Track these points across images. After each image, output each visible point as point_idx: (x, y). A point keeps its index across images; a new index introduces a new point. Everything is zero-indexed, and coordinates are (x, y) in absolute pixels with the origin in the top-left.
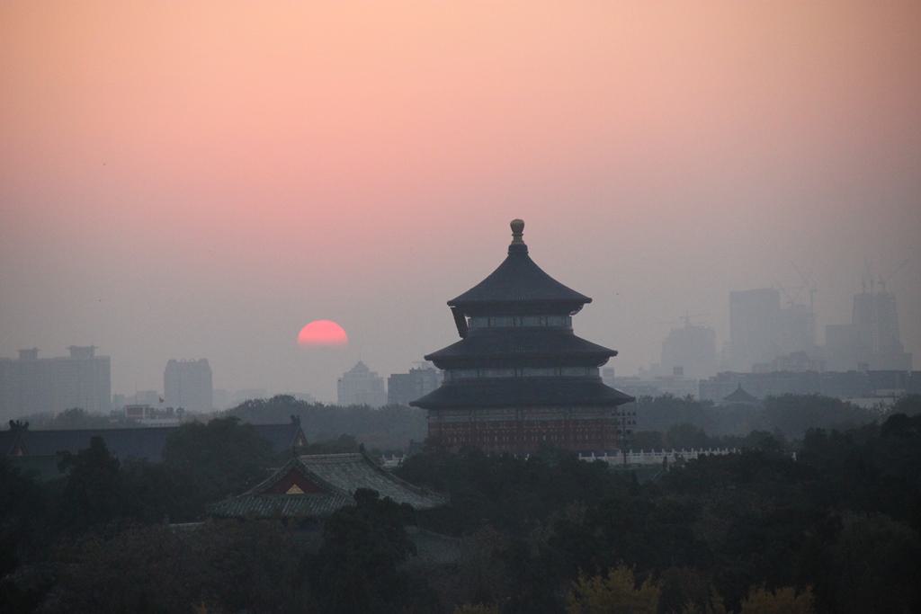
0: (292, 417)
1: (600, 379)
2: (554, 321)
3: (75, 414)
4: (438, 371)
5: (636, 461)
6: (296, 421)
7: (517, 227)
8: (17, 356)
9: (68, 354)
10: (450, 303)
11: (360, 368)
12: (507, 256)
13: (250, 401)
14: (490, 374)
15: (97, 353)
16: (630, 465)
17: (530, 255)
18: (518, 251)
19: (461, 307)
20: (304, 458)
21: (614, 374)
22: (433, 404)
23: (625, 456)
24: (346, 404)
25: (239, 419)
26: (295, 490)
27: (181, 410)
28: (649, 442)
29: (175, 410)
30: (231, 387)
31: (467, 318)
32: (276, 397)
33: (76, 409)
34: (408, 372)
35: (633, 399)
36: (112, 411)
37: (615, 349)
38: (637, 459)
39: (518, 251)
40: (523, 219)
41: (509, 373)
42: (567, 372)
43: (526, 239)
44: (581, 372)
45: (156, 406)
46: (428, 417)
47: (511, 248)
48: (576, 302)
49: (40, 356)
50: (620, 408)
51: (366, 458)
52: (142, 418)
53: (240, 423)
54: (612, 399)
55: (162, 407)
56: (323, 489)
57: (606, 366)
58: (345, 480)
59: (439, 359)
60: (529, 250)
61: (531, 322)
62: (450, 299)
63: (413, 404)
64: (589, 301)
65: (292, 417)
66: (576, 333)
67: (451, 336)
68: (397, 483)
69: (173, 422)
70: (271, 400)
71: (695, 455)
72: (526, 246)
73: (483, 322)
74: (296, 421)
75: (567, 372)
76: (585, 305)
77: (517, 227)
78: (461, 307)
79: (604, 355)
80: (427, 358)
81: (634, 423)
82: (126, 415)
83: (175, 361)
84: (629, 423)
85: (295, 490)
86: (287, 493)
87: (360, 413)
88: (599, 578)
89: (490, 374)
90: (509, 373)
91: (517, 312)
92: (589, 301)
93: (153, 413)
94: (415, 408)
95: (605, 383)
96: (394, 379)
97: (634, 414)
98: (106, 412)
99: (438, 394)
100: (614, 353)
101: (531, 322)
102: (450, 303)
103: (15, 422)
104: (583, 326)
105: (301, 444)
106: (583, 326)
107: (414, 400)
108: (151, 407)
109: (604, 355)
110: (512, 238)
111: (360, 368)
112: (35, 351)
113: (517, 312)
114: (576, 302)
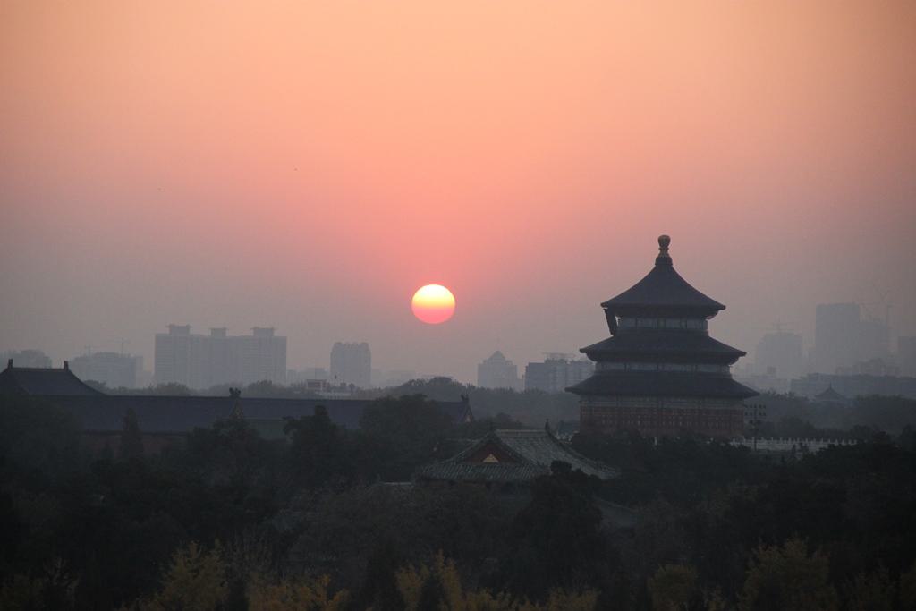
0: (462, 397)
1: (730, 375)
2: (692, 324)
3: (265, 385)
4: (594, 363)
5: (780, 448)
6: (465, 399)
7: (664, 242)
8: (208, 333)
9: (251, 333)
10: (603, 305)
11: (498, 354)
12: (654, 266)
13: (413, 381)
14: (636, 367)
15: (276, 334)
16: (759, 451)
17: (674, 266)
18: (664, 262)
19: (611, 308)
20: (499, 432)
21: (738, 371)
22: (586, 390)
23: (755, 442)
24: (491, 385)
25: (425, 396)
26: (491, 459)
27: (352, 386)
28: (761, 430)
29: (347, 386)
30: (387, 371)
31: (617, 319)
32: (435, 378)
33: (265, 382)
34: (543, 362)
35: (757, 394)
36: (292, 385)
37: (743, 350)
38: (763, 445)
39: (664, 262)
40: (671, 237)
41: (651, 367)
42: (703, 368)
43: (671, 252)
44: (714, 369)
45: (332, 383)
46: (580, 402)
47: (658, 260)
48: (713, 308)
49: (229, 334)
50: (747, 401)
51: (550, 435)
52: (319, 391)
53: (426, 400)
54: (740, 393)
55: (338, 384)
56: (517, 460)
57: (736, 363)
58: (541, 456)
59: (592, 352)
60: (673, 262)
61: (674, 324)
62: (604, 301)
63: (567, 390)
64: (723, 308)
65: (462, 397)
66: (711, 335)
67: (604, 333)
68: (575, 457)
69: (345, 395)
70: (431, 381)
71: (823, 445)
72: (670, 259)
73: (631, 323)
74: (465, 399)
75: (703, 368)
76: (720, 311)
77: (664, 242)
78: (611, 308)
79: (734, 355)
80: (582, 351)
81: (765, 414)
82: (307, 388)
83: (339, 343)
84: (760, 414)
85: (491, 459)
86: (485, 461)
87: (505, 395)
88: (776, 547)
89: (636, 367)
90: (651, 367)
91: (661, 317)
92: (723, 308)
93: (329, 388)
94: (570, 393)
95: (734, 378)
96: (531, 368)
97: (765, 407)
98: (287, 384)
99: (590, 382)
100: (743, 354)
101: (674, 324)
102: (603, 305)
103: (234, 389)
104: (717, 329)
105: (468, 420)
106: (717, 329)
107: (570, 386)
108: (327, 381)
109: (734, 355)
110: (659, 252)
111: (498, 354)
112: (224, 330)
113: (661, 317)
114: (713, 308)
